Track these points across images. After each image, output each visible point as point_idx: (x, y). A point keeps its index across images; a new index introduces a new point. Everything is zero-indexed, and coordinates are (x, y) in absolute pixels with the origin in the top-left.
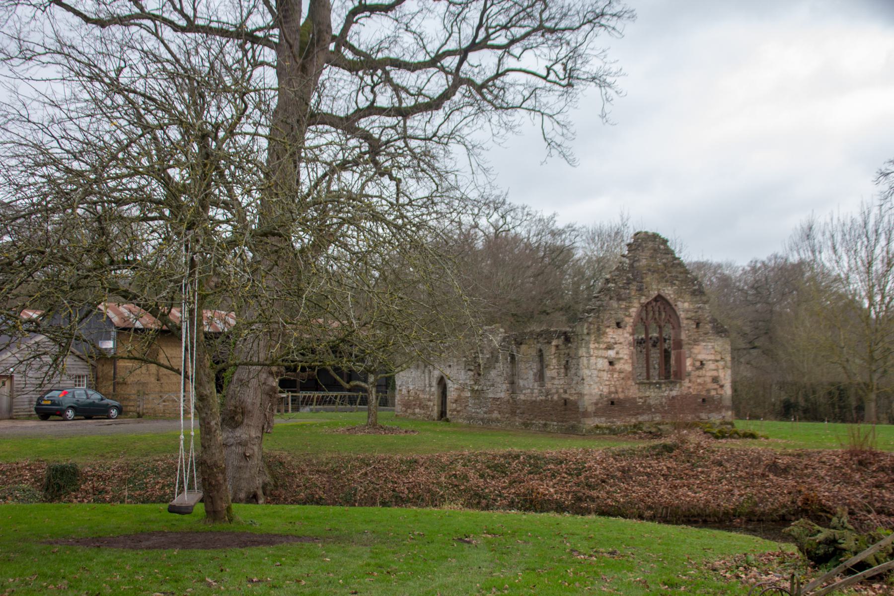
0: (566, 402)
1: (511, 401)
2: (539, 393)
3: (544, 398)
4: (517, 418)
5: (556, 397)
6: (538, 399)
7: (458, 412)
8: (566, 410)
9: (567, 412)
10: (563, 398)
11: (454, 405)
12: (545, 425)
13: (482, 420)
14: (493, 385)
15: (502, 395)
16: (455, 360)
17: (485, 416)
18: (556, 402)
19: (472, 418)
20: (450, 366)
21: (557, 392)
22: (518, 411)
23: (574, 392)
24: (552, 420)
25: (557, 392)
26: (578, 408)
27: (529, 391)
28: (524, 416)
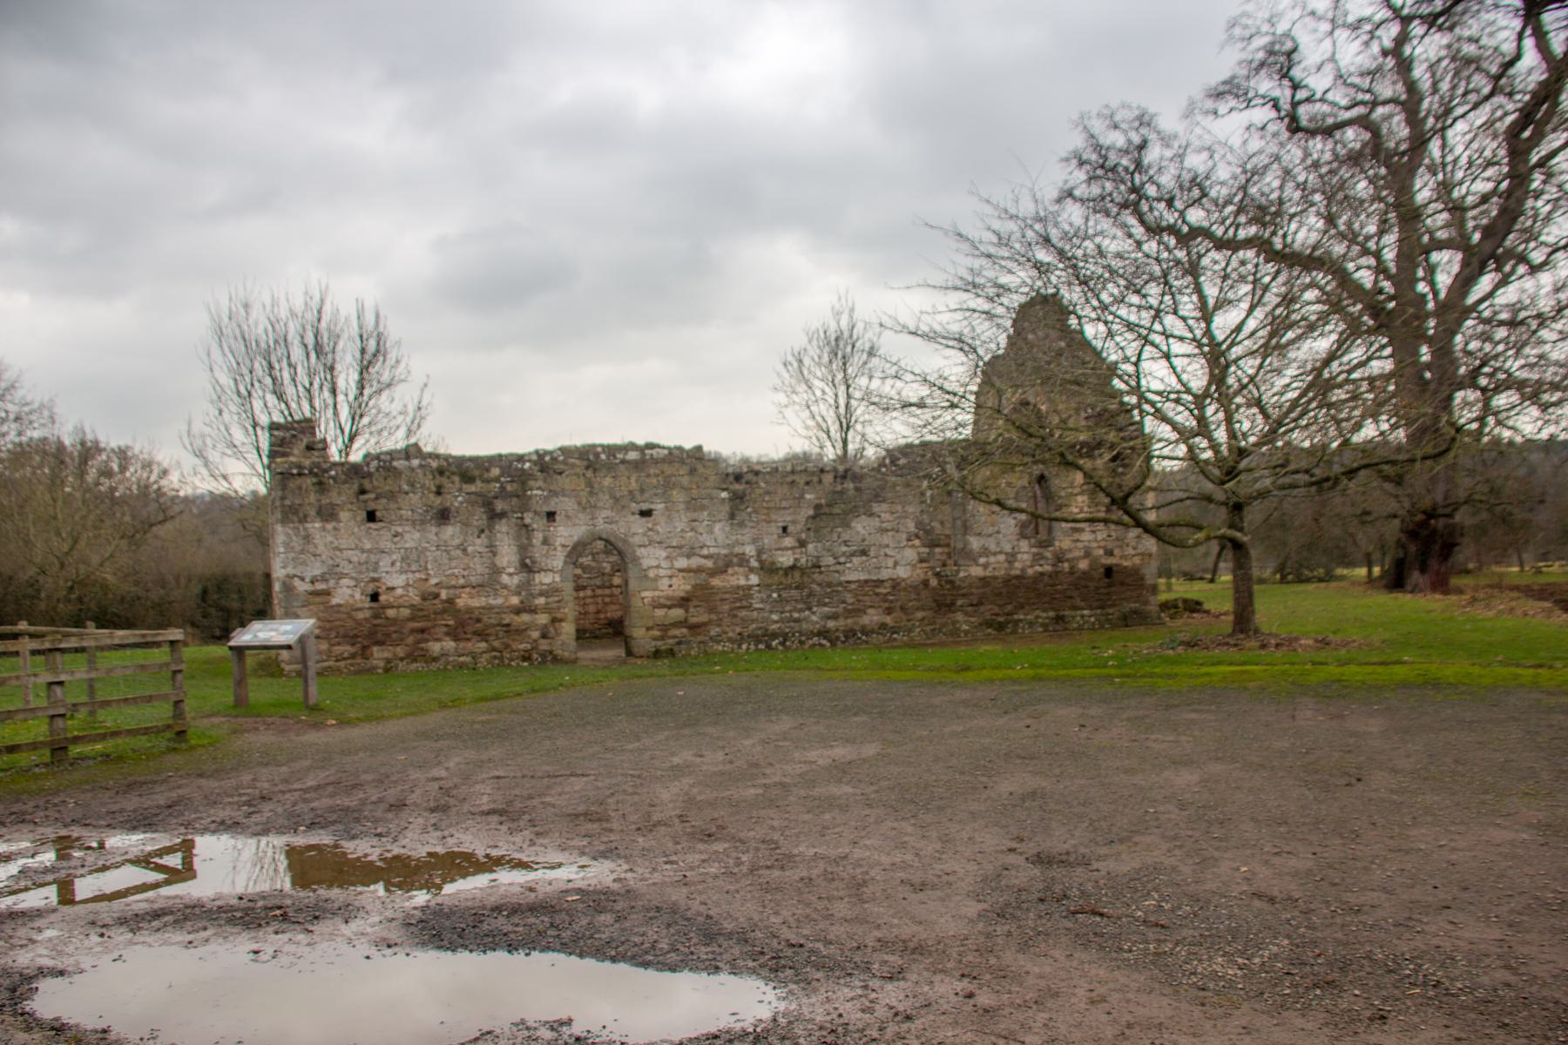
0: (1109, 571)
1: (934, 582)
2: (1033, 560)
3: (1048, 568)
4: (960, 617)
5: (1083, 565)
6: (1030, 571)
7: (694, 628)
8: (1109, 585)
9: (1113, 589)
10: (1103, 565)
11: (677, 613)
12: (1059, 619)
13: (823, 633)
14: (864, 553)
15: (902, 572)
16: (678, 496)
17: (831, 624)
18: (1084, 573)
19: (774, 636)
20: (646, 514)
21: (1087, 554)
22: (959, 602)
23: (1133, 552)
24: (1075, 608)
25: (1087, 554)
26: (1142, 579)
27: (1002, 558)
28: (982, 609)
